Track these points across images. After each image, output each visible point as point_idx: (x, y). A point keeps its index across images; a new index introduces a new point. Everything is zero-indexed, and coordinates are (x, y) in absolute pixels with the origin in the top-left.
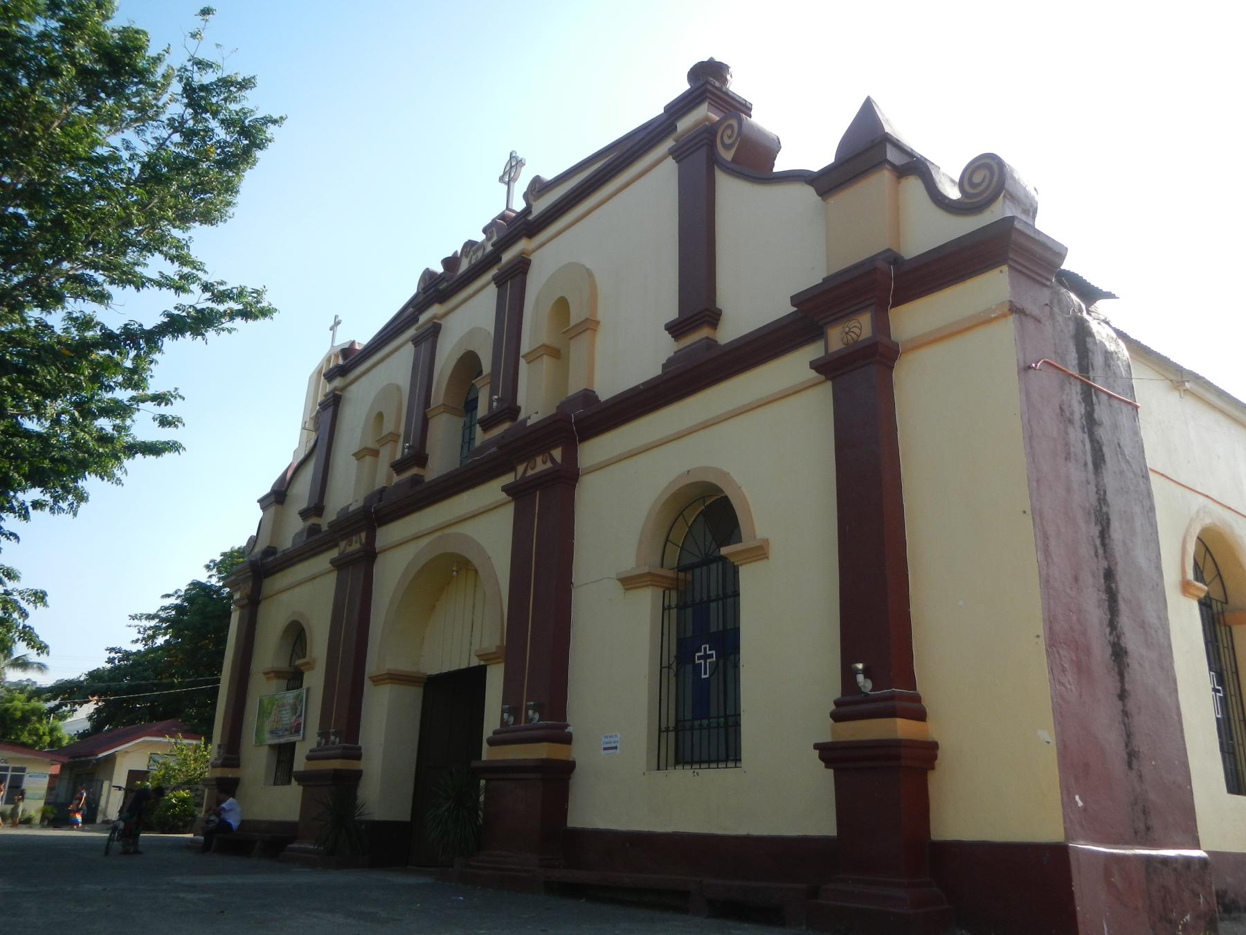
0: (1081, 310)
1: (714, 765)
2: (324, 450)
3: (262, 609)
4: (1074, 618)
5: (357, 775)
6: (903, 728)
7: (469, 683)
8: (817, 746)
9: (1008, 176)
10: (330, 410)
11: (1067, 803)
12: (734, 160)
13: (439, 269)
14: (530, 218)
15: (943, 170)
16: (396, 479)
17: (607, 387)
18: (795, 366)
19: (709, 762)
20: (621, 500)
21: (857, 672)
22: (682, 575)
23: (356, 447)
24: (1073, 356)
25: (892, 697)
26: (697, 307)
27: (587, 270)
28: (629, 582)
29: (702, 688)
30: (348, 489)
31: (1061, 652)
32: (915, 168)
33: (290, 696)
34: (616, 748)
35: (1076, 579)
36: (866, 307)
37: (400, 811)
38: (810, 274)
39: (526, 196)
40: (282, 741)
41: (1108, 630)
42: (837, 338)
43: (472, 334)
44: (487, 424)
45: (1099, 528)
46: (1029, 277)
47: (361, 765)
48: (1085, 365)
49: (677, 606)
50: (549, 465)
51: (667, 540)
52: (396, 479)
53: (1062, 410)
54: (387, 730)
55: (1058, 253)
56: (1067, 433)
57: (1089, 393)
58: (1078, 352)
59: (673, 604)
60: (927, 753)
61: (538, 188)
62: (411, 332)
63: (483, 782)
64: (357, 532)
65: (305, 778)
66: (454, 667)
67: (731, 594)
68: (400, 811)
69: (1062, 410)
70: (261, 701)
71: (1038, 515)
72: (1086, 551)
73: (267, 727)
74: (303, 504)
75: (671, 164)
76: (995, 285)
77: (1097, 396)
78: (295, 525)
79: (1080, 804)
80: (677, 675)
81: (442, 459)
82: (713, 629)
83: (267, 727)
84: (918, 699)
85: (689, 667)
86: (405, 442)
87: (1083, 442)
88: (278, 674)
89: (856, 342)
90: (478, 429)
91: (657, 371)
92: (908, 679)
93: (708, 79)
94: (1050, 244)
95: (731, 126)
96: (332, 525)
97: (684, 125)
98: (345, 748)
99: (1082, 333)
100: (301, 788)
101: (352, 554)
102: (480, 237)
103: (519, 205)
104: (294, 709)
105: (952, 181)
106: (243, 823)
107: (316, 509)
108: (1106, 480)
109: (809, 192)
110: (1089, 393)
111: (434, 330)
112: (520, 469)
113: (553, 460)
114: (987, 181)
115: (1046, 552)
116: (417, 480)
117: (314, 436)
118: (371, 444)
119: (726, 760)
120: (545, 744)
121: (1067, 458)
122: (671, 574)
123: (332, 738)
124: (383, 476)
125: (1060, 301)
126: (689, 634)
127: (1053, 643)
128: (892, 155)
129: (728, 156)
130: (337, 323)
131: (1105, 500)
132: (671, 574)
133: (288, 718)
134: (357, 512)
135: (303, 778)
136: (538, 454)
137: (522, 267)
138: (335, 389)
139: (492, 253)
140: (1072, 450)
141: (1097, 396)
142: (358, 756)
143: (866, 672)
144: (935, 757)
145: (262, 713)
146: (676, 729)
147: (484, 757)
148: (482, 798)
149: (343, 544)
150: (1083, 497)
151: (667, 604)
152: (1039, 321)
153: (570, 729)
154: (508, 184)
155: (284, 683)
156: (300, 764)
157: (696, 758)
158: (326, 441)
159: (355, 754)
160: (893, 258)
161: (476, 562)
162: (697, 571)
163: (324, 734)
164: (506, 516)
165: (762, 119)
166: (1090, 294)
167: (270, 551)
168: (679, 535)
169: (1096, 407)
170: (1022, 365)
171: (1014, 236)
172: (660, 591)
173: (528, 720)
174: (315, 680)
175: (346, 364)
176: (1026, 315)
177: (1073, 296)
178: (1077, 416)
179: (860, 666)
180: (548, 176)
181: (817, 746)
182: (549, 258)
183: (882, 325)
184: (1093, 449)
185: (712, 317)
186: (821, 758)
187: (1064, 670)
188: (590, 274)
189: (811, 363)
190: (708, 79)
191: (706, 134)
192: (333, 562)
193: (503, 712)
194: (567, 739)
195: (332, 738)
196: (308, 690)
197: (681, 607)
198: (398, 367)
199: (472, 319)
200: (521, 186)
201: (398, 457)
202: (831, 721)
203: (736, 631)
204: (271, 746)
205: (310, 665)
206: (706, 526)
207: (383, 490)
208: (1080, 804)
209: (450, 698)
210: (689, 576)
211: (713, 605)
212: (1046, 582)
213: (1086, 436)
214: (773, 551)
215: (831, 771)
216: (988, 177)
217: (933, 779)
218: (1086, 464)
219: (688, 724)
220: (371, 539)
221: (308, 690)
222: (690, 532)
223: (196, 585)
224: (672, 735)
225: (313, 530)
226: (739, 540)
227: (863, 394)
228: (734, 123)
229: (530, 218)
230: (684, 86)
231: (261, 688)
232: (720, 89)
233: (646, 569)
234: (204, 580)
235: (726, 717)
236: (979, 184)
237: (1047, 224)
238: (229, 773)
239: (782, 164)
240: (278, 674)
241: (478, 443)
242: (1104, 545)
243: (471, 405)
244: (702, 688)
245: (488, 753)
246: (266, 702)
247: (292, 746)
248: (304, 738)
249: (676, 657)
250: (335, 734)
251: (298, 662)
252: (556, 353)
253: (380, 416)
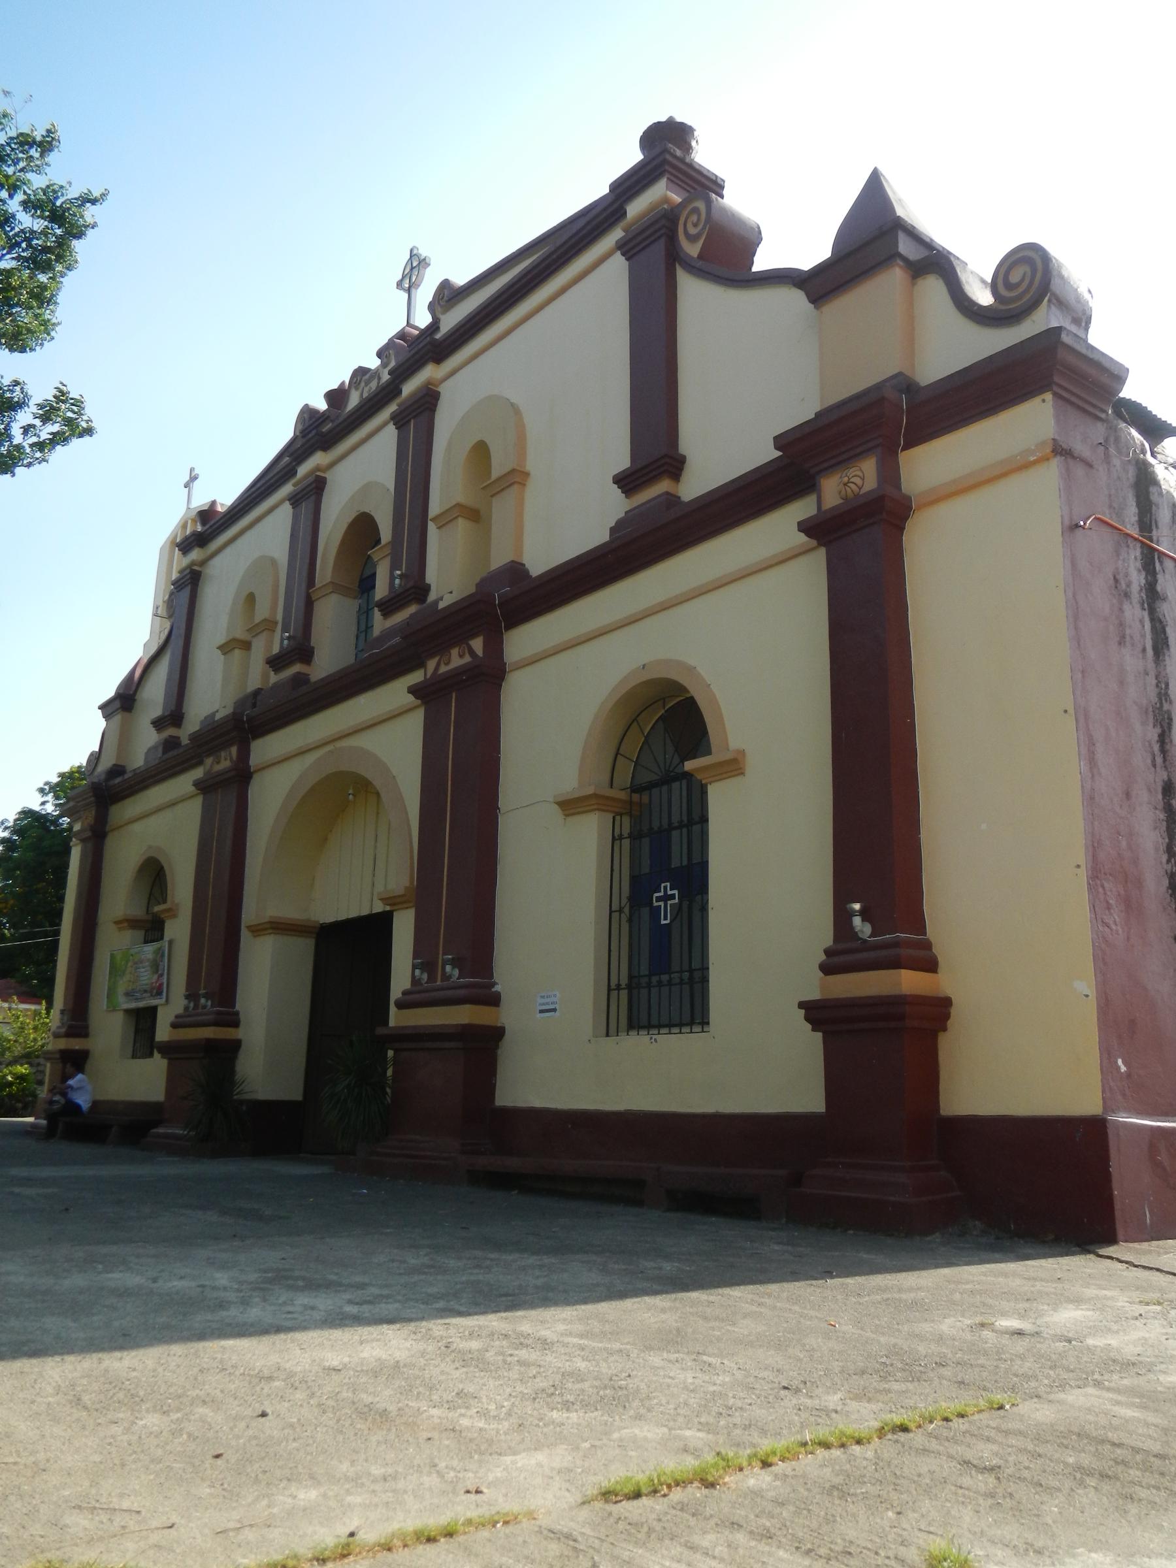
0: (1143, 452)
1: (676, 1030)
2: (181, 642)
3: (111, 843)
4: (1124, 844)
5: (235, 1046)
6: (909, 981)
7: (371, 933)
8: (802, 1005)
9: (1055, 273)
10: (187, 592)
11: (1107, 1068)
12: (700, 256)
13: (322, 405)
14: (438, 336)
15: (970, 267)
16: (274, 678)
17: (540, 558)
18: (779, 528)
19: (670, 1026)
20: (559, 700)
21: (852, 913)
22: (636, 797)
23: (221, 639)
24: (1132, 511)
25: (896, 944)
26: (655, 452)
27: (512, 405)
28: (570, 806)
29: (661, 937)
30: (212, 695)
31: (1106, 885)
32: (936, 264)
33: (149, 950)
34: (554, 1010)
35: (1128, 795)
36: (869, 450)
37: (295, 1092)
38: (799, 407)
39: (431, 307)
40: (141, 1004)
41: (1165, 858)
42: (833, 490)
43: (367, 489)
44: (389, 607)
45: (1158, 730)
46: (1079, 407)
47: (240, 1033)
48: (1146, 522)
49: (630, 836)
50: (467, 659)
51: (617, 754)
52: (274, 678)
53: (1116, 580)
54: (271, 993)
55: (1118, 376)
56: (1121, 610)
57: (1150, 559)
58: (1138, 505)
59: (626, 832)
60: (936, 1012)
61: (447, 295)
62: (287, 489)
63: (390, 1053)
64: (226, 745)
65: (167, 1049)
66: (353, 913)
67: (697, 819)
68: (295, 1092)
69: (1116, 580)
70: (112, 956)
71: (1083, 716)
72: (1141, 760)
73: (122, 986)
74: (157, 712)
75: (619, 262)
76: (1033, 420)
77: (1161, 563)
78: (147, 738)
79: (1123, 1069)
80: (630, 920)
81: (331, 654)
82: (675, 863)
83: (122, 986)
84: (928, 945)
85: (645, 911)
86: (284, 630)
87: (1142, 621)
88: (133, 923)
89: (857, 496)
90: (377, 614)
91: (604, 537)
92: (917, 922)
93: (666, 144)
94: (1107, 364)
95: (696, 211)
96: (194, 737)
97: (636, 208)
98: (219, 1013)
99: (1145, 481)
100: (165, 1062)
101: (220, 774)
102: (374, 363)
103: (423, 319)
104: (155, 966)
105: (983, 281)
106: (95, 1104)
107: (173, 717)
108: (1169, 669)
109: (797, 298)
110: (1150, 559)
111: (317, 487)
112: (431, 664)
113: (472, 652)
114: (1027, 282)
115: (1092, 762)
116: (300, 680)
117: (168, 625)
118: (240, 634)
119: (691, 1023)
120: (468, 1006)
121: (1121, 642)
122: (623, 795)
123: (203, 1001)
124: (257, 675)
125: (1117, 440)
126: (646, 869)
127: (1096, 874)
128: (905, 246)
129: (692, 250)
130: (193, 478)
131: (1166, 694)
132: (623, 795)
133: (146, 977)
134: (225, 720)
135: (167, 1049)
136: (452, 646)
137: (428, 400)
138: (193, 563)
139: (388, 384)
140: (1128, 631)
141: (1161, 563)
142: (235, 1024)
143: (864, 914)
144: (947, 1016)
145: (115, 971)
146: (629, 987)
147: (392, 1023)
148: (390, 1072)
149: (209, 761)
150: (1139, 693)
151: (617, 832)
152: (1090, 466)
153: (497, 988)
154: (409, 291)
155: (140, 934)
156: (163, 1033)
157: (654, 1021)
158: (183, 631)
159: (233, 1021)
160: (905, 384)
161: (378, 783)
162: (655, 791)
163: (192, 996)
164: (415, 723)
165: (739, 199)
166: (1156, 430)
167: (117, 771)
168: (633, 746)
169: (1160, 577)
170: (1067, 522)
171: (1061, 354)
172: (610, 816)
173: (446, 977)
174: (179, 930)
175: (207, 530)
176: (1074, 457)
177: (1134, 433)
178: (1135, 588)
179: (857, 906)
180: (460, 279)
181: (802, 1005)
182: (463, 390)
183: (890, 473)
184: (1153, 628)
185: (674, 465)
186: (807, 1019)
187: (1109, 907)
188: (515, 410)
189: (799, 523)
190: (666, 144)
191: (661, 222)
192: (197, 784)
193: (414, 967)
194: (494, 1001)
195: (203, 1001)
196: (171, 942)
197: (635, 837)
198: (272, 533)
199: (365, 471)
200: (426, 293)
201: (276, 649)
202: (821, 974)
203: (704, 866)
204: (127, 1011)
205: (173, 913)
206: (666, 736)
207: (257, 693)
208: (1123, 1069)
209: (349, 952)
210: (645, 798)
211: (675, 834)
212: (1090, 799)
213: (1146, 614)
214: (753, 763)
215: (820, 1035)
216: (1030, 276)
217: (946, 1043)
218: (1144, 650)
219: (644, 981)
220: (244, 754)
221: (171, 942)
222: (646, 742)
223: (27, 813)
224: (624, 994)
225: (170, 744)
226: (708, 752)
227: (864, 560)
228: (701, 205)
229: (438, 336)
230: (635, 156)
231: (112, 941)
232: (682, 161)
233: (590, 791)
234: (37, 808)
235: (691, 971)
236: (1018, 285)
237: (1103, 337)
238: (76, 1044)
239: (762, 262)
240: (133, 923)
241: (377, 631)
242: (1163, 751)
243: (367, 584)
244: (661, 937)
245: (396, 1018)
246: (118, 958)
247: (153, 1011)
248: (167, 1000)
249: (630, 899)
250: (206, 996)
251: (157, 909)
252: (474, 515)
253: (251, 599)
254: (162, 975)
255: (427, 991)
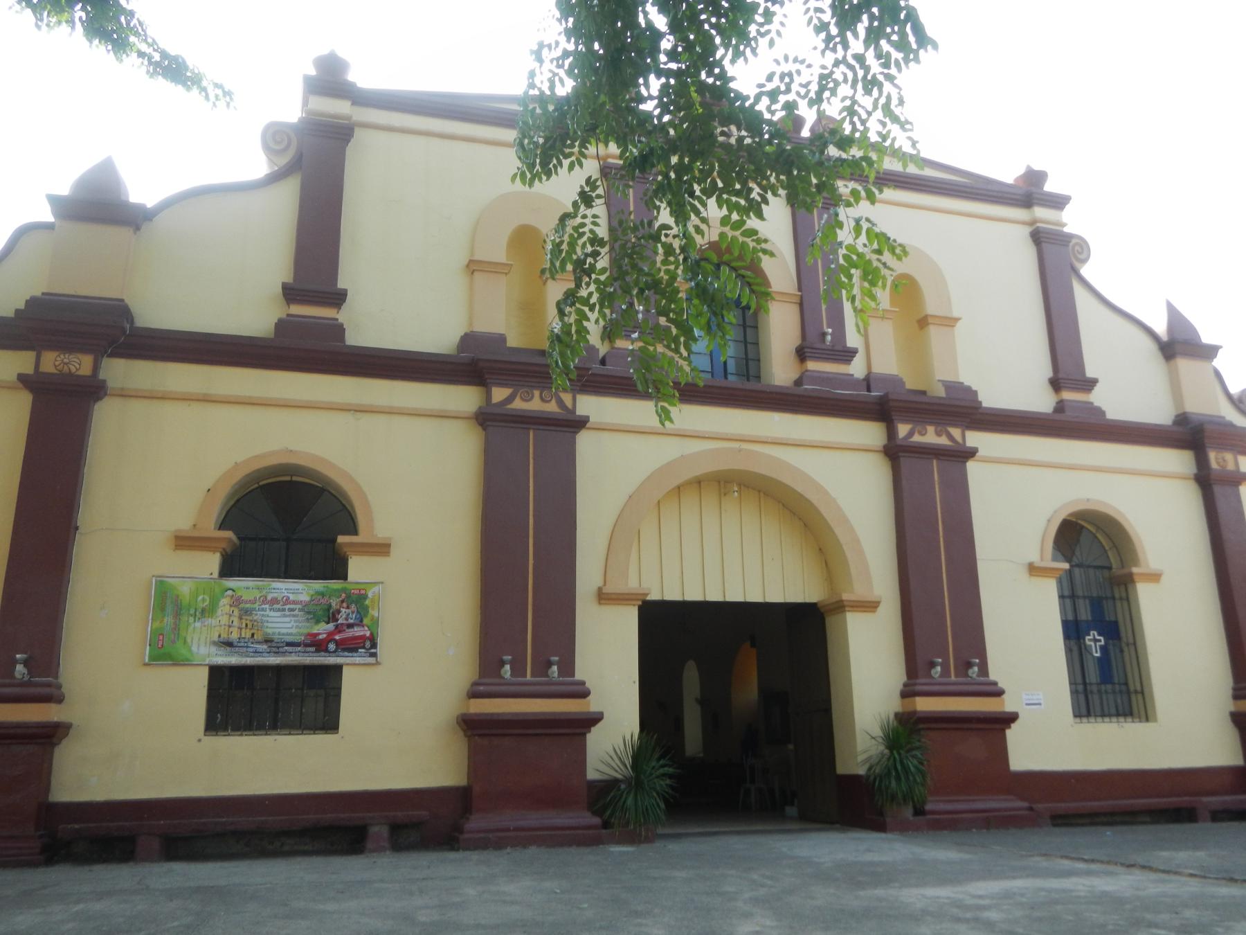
26: (1067, 371)
28: (1033, 570)
33: (300, 590)
95: (1081, 247)
113: (951, 437)
133: (285, 625)
136: (931, 423)
138: (349, 118)
214: (1164, 578)
235: (1085, 684)
246: (185, 589)
254: (360, 623)
255: (940, 684)
